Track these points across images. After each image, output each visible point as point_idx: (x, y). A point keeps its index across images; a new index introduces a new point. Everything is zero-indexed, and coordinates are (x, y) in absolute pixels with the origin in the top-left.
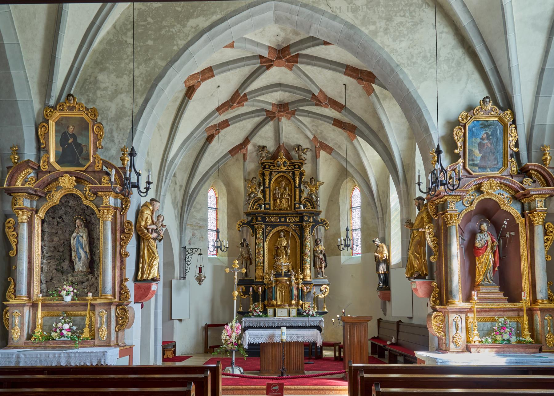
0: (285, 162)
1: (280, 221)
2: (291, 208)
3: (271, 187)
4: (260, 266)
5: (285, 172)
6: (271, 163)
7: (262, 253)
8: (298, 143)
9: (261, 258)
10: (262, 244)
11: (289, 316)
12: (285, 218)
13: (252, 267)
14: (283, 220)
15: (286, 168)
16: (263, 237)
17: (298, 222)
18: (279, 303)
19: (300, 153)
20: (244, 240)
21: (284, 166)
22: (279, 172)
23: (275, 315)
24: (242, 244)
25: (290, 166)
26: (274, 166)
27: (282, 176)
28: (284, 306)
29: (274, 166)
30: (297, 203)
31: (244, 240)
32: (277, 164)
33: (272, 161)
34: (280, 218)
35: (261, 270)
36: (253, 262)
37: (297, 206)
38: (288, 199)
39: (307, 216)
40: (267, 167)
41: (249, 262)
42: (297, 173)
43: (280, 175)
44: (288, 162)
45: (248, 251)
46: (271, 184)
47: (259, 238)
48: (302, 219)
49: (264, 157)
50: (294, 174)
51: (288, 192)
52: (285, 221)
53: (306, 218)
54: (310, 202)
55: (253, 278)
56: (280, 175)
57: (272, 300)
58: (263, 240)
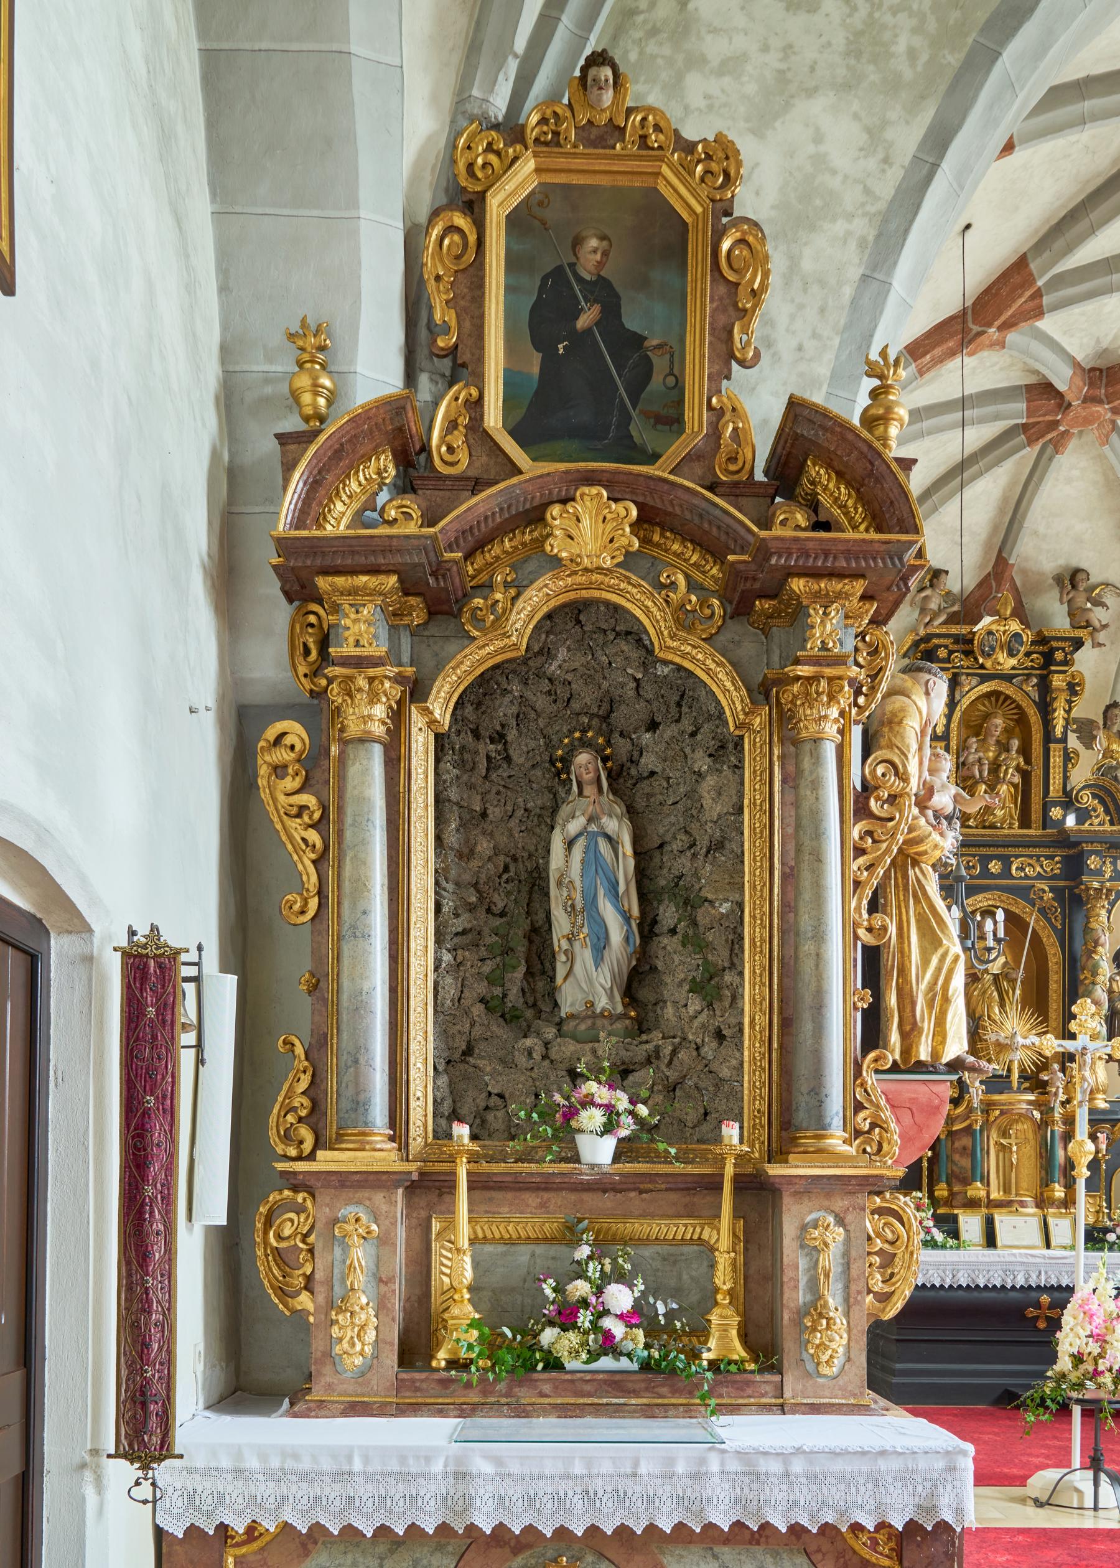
0: (1017, 635)
1: (986, 873)
2: (1025, 822)
3: (954, 735)
5: (1008, 678)
8: (1076, 563)
11: (1048, 1246)
12: (1006, 861)
14: (995, 867)
15: (1013, 662)
17: (1054, 877)
18: (995, 1195)
19: (1080, 600)
22: (984, 679)
23: (991, 1241)
27: (996, 694)
28: (1022, 1204)
30: (1055, 804)
34: (985, 860)
37: (1056, 813)
38: (1015, 786)
39: (1096, 853)
40: (942, 653)
42: (1058, 681)
43: (985, 688)
46: (954, 725)
48: (1074, 866)
49: (935, 615)
50: (1044, 686)
51: (1015, 759)
52: (1006, 873)
53: (1093, 862)
54: (1102, 801)
56: (985, 688)
57: (967, 1182)
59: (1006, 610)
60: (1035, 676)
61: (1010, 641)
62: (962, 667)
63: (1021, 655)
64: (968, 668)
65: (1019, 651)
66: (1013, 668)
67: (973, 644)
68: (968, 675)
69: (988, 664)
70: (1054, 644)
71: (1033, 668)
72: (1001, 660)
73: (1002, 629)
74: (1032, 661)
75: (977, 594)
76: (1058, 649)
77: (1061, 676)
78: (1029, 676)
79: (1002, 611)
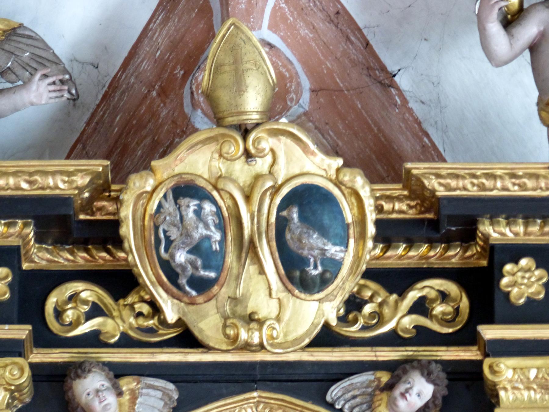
0: (308, 200)
6: (54, 219)
21: (299, 275)
25: (398, 281)
26: (121, 283)
29: (121, 283)
32: (159, 244)
33: (67, 179)
44: (363, 198)
59: (239, 87)
60: (425, 369)
61: (282, 225)
62: (94, 340)
63: (345, 284)
64: (126, 342)
65: (332, 267)
66: (326, 337)
67: (119, 242)
68: (118, 372)
69: (208, 323)
70: (497, 232)
71: (424, 336)
72: (262, 305)
73: (242, 172)
74: (421, 307)
75: (161, 39)
76: (515, 252)
77: (534, 366)
78: (397, 370)
79: (224, 97)
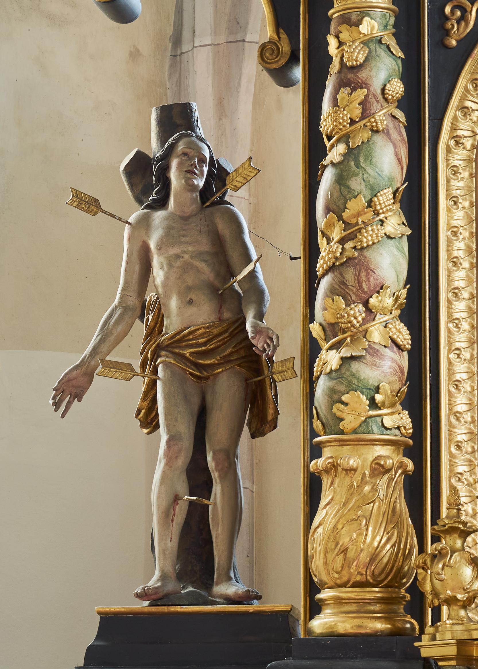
4: (360, 437)
7: (390, 264)
9: (388, 329)
10: (388, 160)
13: (273, 462)
16: (411, 73)
20: (176, 119)
24: (147, 177)
31: (176, 119)
35: (389, 492)
36: (288, 394)
41: (226, 391)
45: (225, 252)
47: (351, 77)
55: (284, 595)
58: (410, 103)
